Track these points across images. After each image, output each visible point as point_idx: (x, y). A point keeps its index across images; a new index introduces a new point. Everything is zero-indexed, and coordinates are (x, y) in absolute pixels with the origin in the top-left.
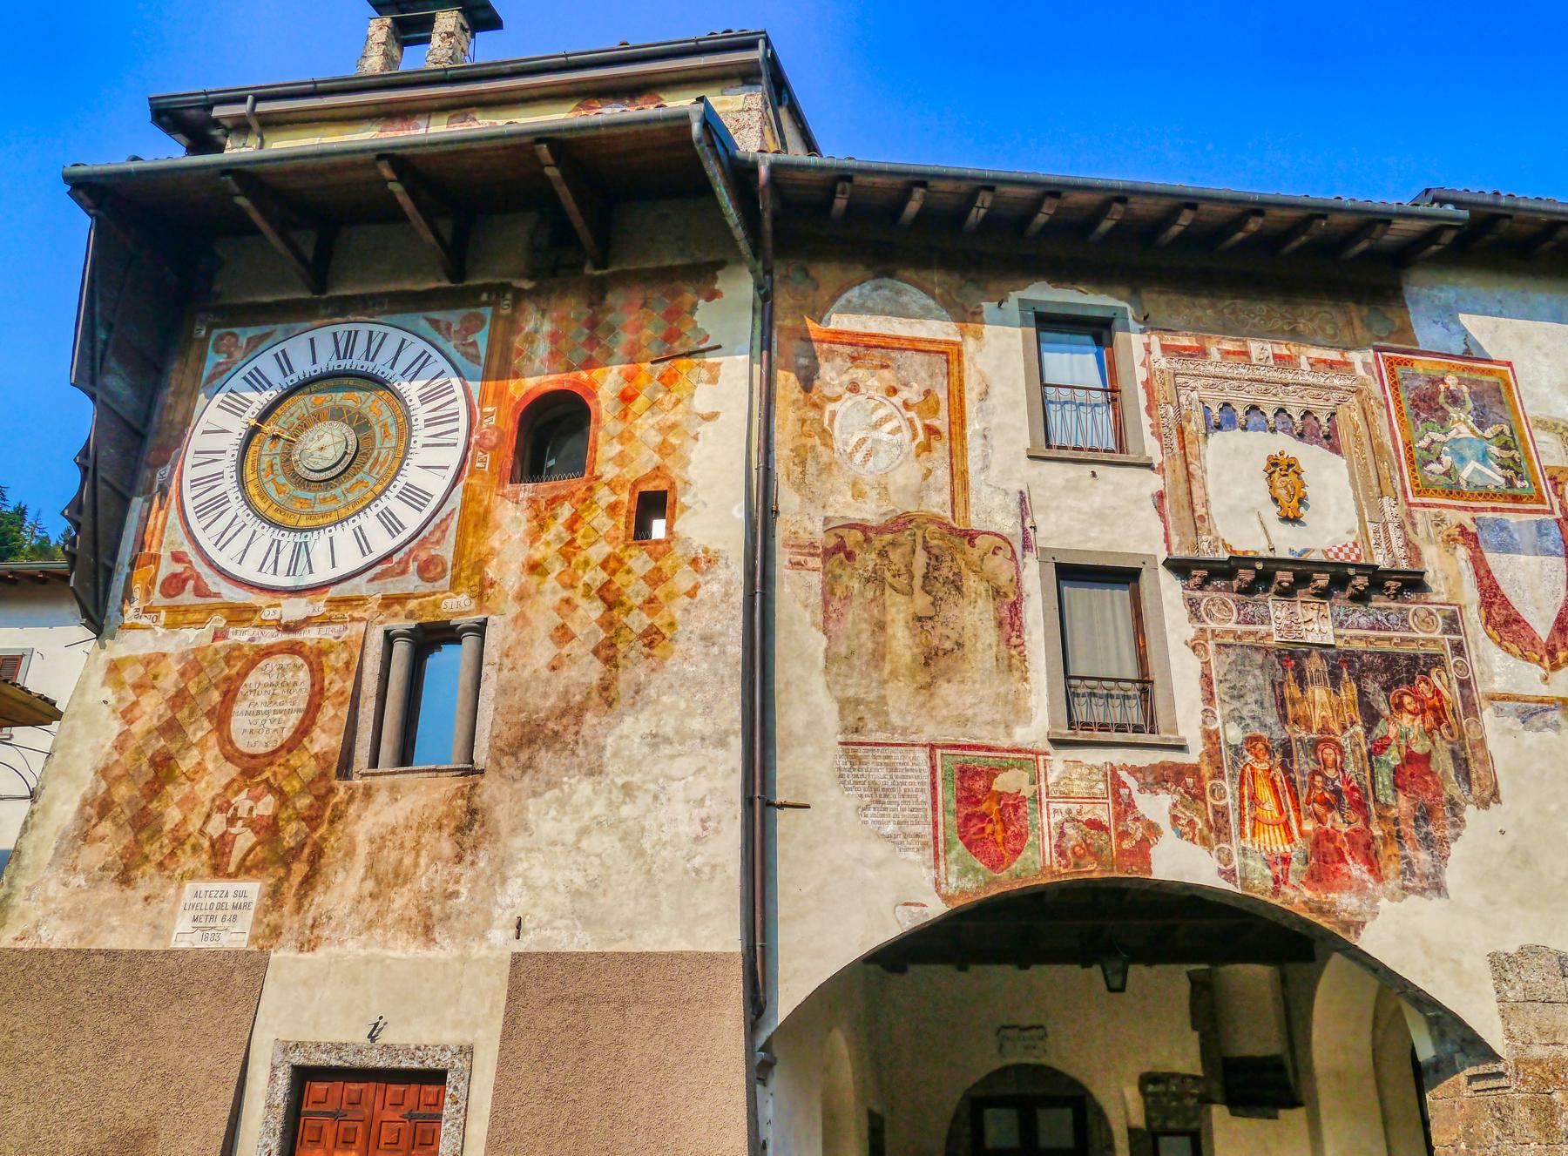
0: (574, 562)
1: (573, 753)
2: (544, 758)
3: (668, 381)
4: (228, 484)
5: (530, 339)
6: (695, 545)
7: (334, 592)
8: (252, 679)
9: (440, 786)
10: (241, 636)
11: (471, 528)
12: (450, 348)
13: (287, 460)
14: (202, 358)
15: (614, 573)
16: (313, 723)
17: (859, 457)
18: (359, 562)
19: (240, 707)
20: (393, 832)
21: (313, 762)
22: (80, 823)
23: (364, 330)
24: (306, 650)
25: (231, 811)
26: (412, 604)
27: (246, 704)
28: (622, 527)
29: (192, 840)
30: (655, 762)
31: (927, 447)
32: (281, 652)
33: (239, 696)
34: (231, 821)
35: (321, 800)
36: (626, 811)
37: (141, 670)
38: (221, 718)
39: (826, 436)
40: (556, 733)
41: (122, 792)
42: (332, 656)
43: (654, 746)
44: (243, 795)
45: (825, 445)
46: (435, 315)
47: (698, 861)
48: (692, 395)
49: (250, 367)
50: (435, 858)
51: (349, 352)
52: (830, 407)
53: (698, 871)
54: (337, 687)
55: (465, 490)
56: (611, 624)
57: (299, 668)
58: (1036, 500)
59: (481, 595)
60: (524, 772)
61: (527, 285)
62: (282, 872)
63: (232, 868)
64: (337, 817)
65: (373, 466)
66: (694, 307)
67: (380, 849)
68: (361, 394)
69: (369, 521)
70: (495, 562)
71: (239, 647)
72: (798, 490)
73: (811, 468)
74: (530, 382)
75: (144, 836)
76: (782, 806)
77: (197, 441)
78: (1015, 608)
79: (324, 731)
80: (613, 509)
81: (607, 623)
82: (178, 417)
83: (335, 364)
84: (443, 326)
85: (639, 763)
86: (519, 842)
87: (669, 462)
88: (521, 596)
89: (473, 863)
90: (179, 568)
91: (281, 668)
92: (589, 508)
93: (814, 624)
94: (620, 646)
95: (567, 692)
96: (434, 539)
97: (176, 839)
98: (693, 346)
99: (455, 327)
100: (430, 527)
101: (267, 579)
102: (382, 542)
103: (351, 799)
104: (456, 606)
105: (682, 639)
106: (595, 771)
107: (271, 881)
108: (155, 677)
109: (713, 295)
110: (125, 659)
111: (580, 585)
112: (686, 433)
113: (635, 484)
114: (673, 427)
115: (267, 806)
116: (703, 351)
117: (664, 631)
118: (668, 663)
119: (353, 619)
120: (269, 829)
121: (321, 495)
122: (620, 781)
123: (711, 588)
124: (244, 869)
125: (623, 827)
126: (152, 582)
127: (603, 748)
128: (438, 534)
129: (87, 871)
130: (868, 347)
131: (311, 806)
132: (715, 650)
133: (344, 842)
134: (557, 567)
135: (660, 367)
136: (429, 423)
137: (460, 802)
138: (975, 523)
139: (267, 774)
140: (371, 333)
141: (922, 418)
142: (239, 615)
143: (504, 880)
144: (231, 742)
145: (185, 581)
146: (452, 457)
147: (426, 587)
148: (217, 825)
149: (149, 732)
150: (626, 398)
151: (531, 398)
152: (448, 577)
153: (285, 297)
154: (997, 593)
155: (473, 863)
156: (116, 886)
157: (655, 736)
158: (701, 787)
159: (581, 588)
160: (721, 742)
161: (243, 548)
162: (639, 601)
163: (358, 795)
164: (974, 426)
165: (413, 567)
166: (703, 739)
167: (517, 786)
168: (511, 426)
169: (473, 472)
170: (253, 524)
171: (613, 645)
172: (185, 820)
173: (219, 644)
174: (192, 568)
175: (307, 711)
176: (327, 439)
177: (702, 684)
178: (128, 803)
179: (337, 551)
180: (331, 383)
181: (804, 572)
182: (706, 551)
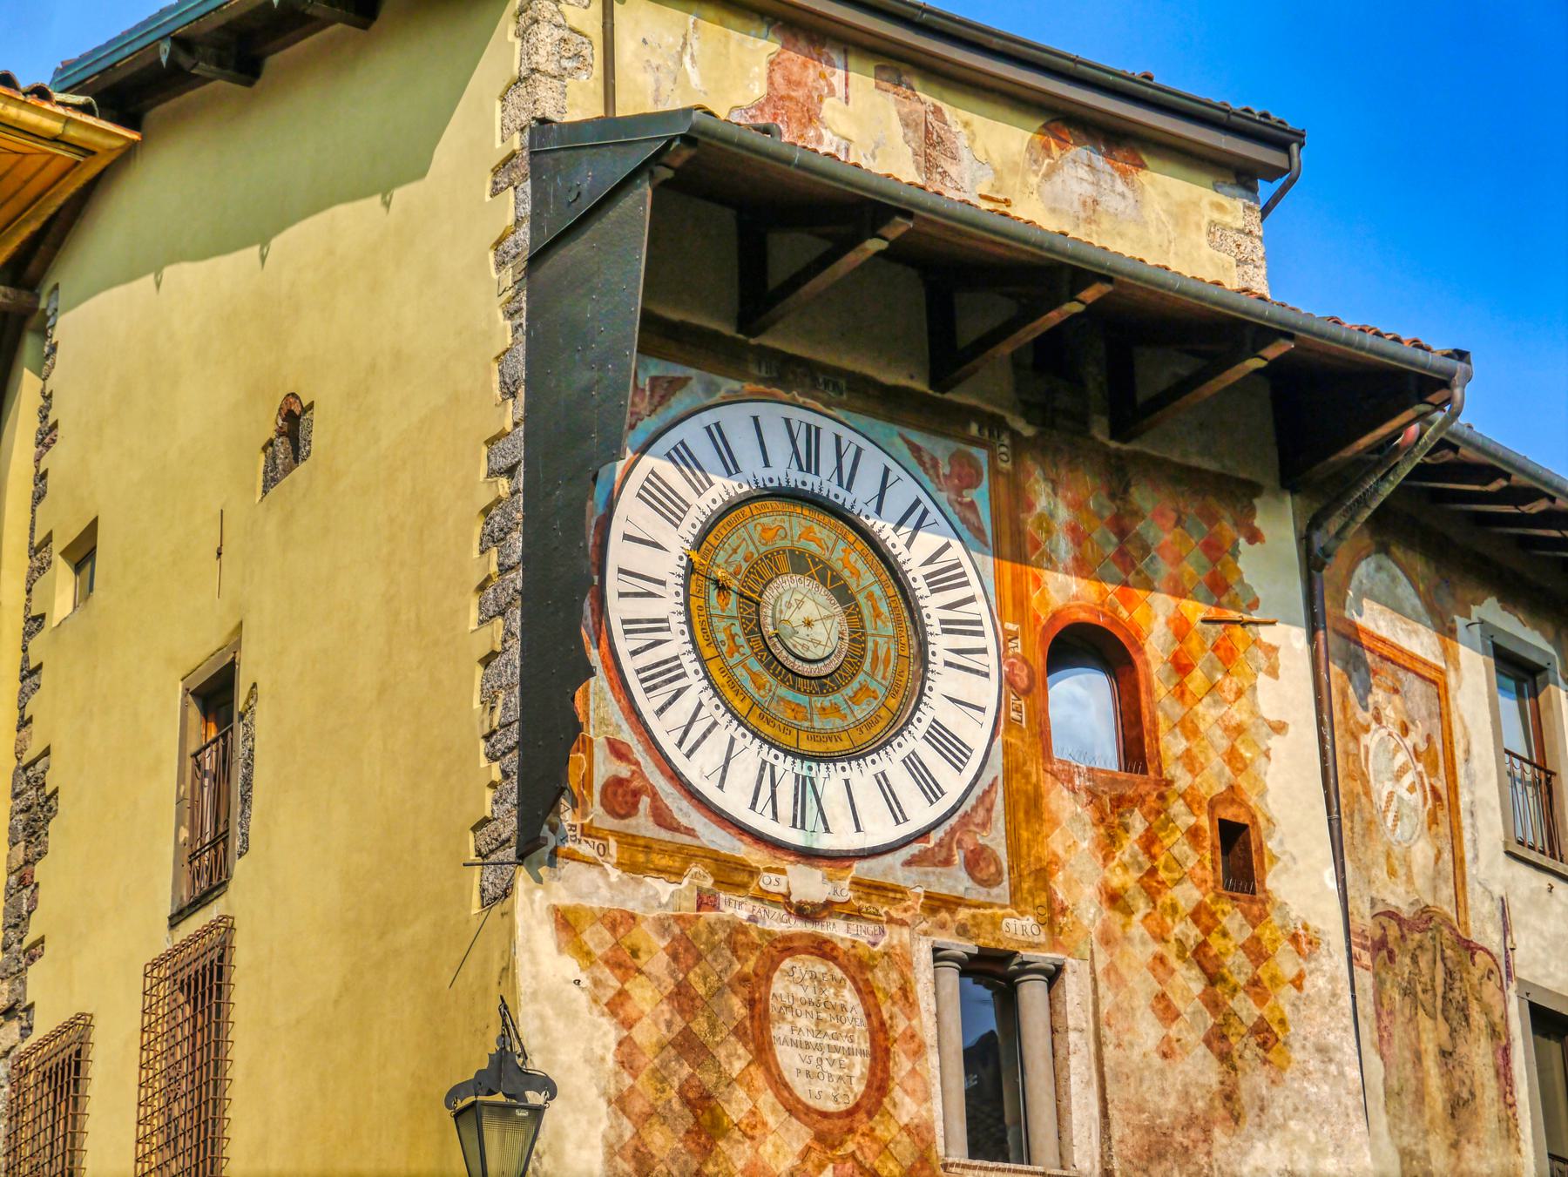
0: (1159, 903)
4: (676, 644)
6: (1293, 915)
7: (859, 869)
10: (736, 909)
11: (1021, 815)
12: (942, 497)
15: (1207, 931)
17: (1391, 816)
18: (893, 833)
19: (780, 1031)
21: (906, 1139)
23: (829, 429)
26: (963, 914)
27: (786, 1028)
31: (1433, 820)
32: (806, 951)
33: (773, 1013)
37: (607, 935)
40: (1186, 1149)
42: (879, 974)
46: (917, 438)
48: (1254, 688)
52: (1365, 739)
57: (840, 984)
58: (1513, 914)
61: (1028, 431)
70: (1060, 876)
78: (1506, 1051)
80: (1194, 834)
81: (1213, 1004)
83: (796, 478)
84: (926, 459)
87: (1242, 781)
90: (624, 771)
91: (814, 977)
92: (1164, 827)
94: (1233, 1040)
95: (1187, 1093)
99: (945, 469)
101: (761, 822)
102: (921, 814)
104: (1019, 930)
105: (1297, 1045)
108: (635, 953)
109: (1254, 537)
112: (1256, 744)
113: (1213, 805)
114: (1239, 730)
117: (1276, 1029)
118: (1287, 1075)
119: (891, 920)
123: (1317, 983)
126: (587, 782)
128: (981, 812)
132: (1333, 1068)
134: (1142, 907)
136: (949, 627)
138: (1474, 937)
139: (850, 1147)
140: (838, 438)
141: (1429, 776)
142: (731, 874)
144: (786, 1085)
145: (636, 794)
150: (1181, 667)
151: (1059, 626)
152: (1006, 883)
154: (1494, 1033)
159: (1173, 946)
162: (1242, 980)
164: (1464, 799)
165: (958, 857)
169: (1009, 721)
170: (727, 729)
171: (1224, 1037)
173: (711, 915)
174: (642, 775)
177: (1326, 1112)
182: (1306, 928)
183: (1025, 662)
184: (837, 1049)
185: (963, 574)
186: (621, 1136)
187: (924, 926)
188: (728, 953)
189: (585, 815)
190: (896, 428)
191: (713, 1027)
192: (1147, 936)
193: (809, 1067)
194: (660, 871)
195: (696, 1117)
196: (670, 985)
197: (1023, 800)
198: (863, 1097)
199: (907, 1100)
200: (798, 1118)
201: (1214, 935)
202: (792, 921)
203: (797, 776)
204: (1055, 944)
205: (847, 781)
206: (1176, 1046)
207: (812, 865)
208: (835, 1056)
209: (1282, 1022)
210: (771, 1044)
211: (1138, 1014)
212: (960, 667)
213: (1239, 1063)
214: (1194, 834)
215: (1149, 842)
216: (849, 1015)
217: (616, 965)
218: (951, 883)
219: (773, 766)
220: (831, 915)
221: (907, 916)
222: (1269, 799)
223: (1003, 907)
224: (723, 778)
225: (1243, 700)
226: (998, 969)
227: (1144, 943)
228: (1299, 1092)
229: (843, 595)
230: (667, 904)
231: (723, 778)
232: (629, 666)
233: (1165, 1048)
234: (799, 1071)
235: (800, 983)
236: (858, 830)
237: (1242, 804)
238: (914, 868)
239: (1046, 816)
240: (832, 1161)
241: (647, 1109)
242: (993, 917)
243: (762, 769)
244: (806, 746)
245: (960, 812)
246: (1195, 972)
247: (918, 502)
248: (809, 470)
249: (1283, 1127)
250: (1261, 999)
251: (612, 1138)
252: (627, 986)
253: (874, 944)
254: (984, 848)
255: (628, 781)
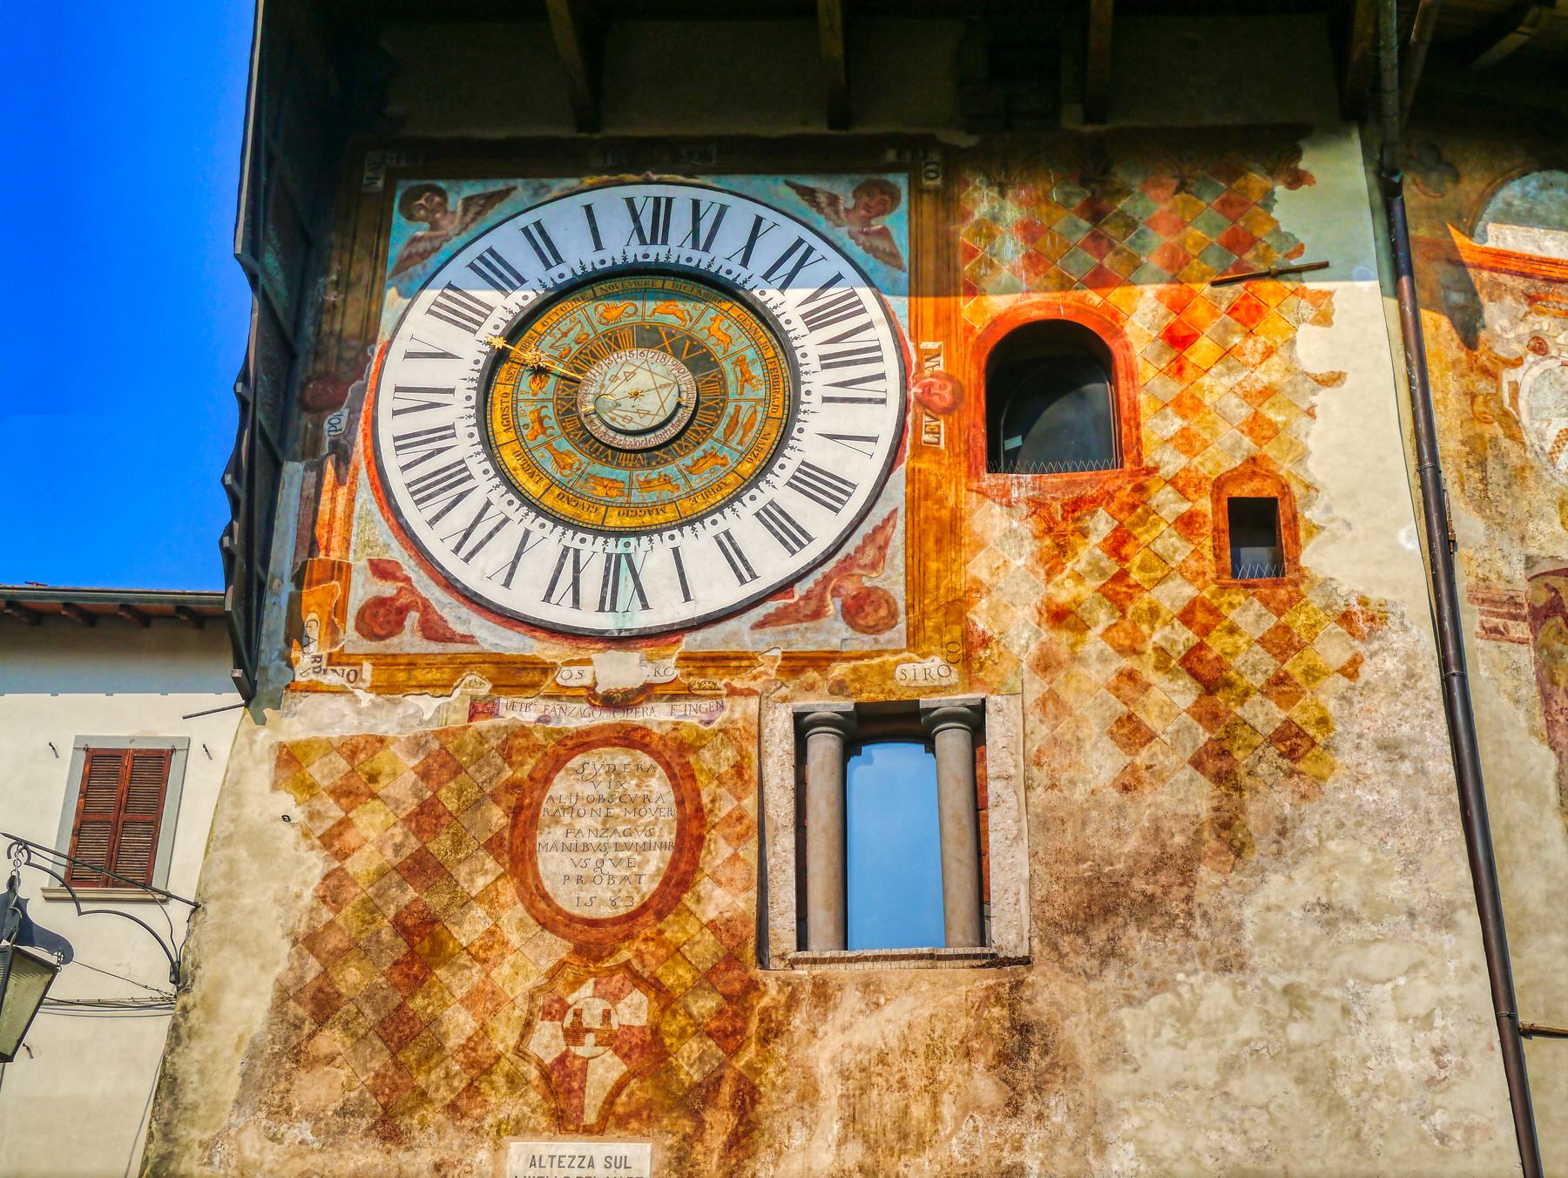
0: (1130, 610)
1: (1188, 934)
2: (1136, 940)
3: (1248, 315)
4: (465, 447)
5: (987, 230)
6: (1343, 590)
7: (690, 642)
8: (561, 787)
9: (956, 983)
10: (522, 712)
11: (930, 545)
12: (841, 235)
13: (568, 409)
14: (383, 228)
15: (1205, 631)
16: (695, 866)
18: (734, 593)
19: (549, 836)
20: (882, 1059)
21: (709, 937)
22: (282, 1030)
23: (682, 196)
24: (656, 744)
25: (569, 1019)
26: (839, 670)
27: (558, 833)
28: (1210, 556)
29: (505, 1065)
30: (1336, 951)
32: (607, 743)
34: (575, 1034)
35: (740, 998)
36: (1296, 1032)
37: (343, 765)
38: (516, 852)
39: (1510, 423)
41: (351, 977)
42: (707, 754)
43: (1331, 924)
44: (587, 990)
45: (1512, 437)
46: (809, 182)
47: (1439, 1118)
48: (1293, 342)
49: (479, 247)
50: (969, 1108)
51: (660, 231)
52: (1508, 376)
53: (1443, 1138)
54: (726, 807)
55: (911, 477)
56: (1215, 717)
57: (647, 772)
59: (967, 659)
60: (1104, 963)
61: (966, 141)
62: (688, 1126)
63: (590, 1117)
64: (772, 1033)
65: (731, 429)
66: (1268, 199)
67: (863, 1090)
68: (689, 306)
69: (743, 523)
70: (984, 603)
71: (524, 732)
72: (1480, 510)
73: (1495, 474)
74: (998, 303)
75: (410, 1055)
76: (1532, 1032)
77: (396, 371)
79: (719, 883)
80: (1187, 524)
82: (351, 324)
83: (636, 252)
84: (822, 199)
85: (1307, 953)
86: (1116, 1082)
87: (1270, 450)
88: (1045, 664)
89: (1040, 1117)
90: (388, 589)
91: (613, 771)
92: (1142, 521)
93: (1533, 732)
94: (1238, 755)
95: (1158, 829)
96: (866, 559)
97: (472, 1064)
98: (1278, 260)
100: (856, 540)
101: (561, 613)
102: (774, 564)
103: (792, 1002)
104: (923, 675)
106: (1231, 964)
107: (670, 1140)
108: (373, 778)
109: (1298, 180)
110: (308, 743)
111: (1149, 650)
112: (1292, 404)
113: (1219, 485)
114: (1268, 392)
115: (634, 1010)
116: (1298, 270)
117: (1311, 732)
118: (1329, 785)
119: (733, 692)
120: (649, 1051)
121: (641, 475)
122: (1278, 982)
123: (1383, 665)
124: (612, 1120)
125: (1297, 1059)
126: (340, 610)
127: (1240, 926)
128: (871, 551)
129: (314, 1117)
130: (1549, 280)
131: (720, 1012)
132: (1406, 767)
133: (794, 1076)
134: (1103, 618)
135: (1230, 293)
136: (828, 362)
137: (996, 1011)
139: (625, 954)
140: (696, 204)
143: (1102, 1147)
144: (545, 897)
145: (402, 612)
146: (883, 422)
147: (863, 643)
148: (547, 1041)
149: (382, 873)
151: (1002, 332)
152: (902, 625)
153: (523, 132)
155: (1040, 1117)
156: (374, 1143)
157: (1328, 907)
158: (1423, 995)
159: (1150, 657)
160: (1445, 921)
161: (516, 562)
162: (1259, 680)
163: (805, 994)
165: (833, 606)
166: (1412, 915)
167: (1094, 986)
168: (972, 375)
170: (521, 520)
171: (1225, 753)
172: (484, 1031)
173: (483, 724)
174: (413, 591)
175: (679, 847)
176: (642, 379)
177: (1393, 823)
178: (368, 998)
179: (692, 572)
180: (629, 283)
181: (1506, 646)
182: (1364, 602)
183: (950, 378)
184: (627, 847)
185: (859, 302)
186: (301, 978)
187: (784, 691)
188: (499, 761)
189: (334, 643)
190: (781, 178)
191: (458, 843)
192: (1110, 650)
193: (582, 872)
194: (423, 687)
195: (411, 946)
196: (411, 804)
197: (934, 528)
198: (653, 896)
199: (718, 892)
200: (554, 932)
201: (1214, 634)
202: (597, 713)
203: (609, 557)
204: (970, 681)
205: (676, 551)
206: (1145, 774)
207: (627, 649)
208: (623, 854)
209: (1323, 722)
210: (532, 853)
211: (1088, 746)
212: (844, 400)
213: (1248, 781)
214: (1187, 524)
215: (1118, 544)
216: (653, 806)
217: (345, 793)
218: (821, 637)
219: (577, 551)
220: (649, 699)
221: (757, 685)
222: (1311, 463)
223: (896, 652)
224: (511, 575)
225: (1275, 359)
226: (913, 727)
227: (1103, 659)
228: (1345, 804)
229: (613, 342)
230: (430, 721)
231: (511, 575)
232: (398, 483)
233: (1127, 780)
234: (567, 878)
235: (592, 780)
236: (687, 597)
237: (1269, 475)
238: (768, 630)
239: (966, 540)
240: (595, 975)
241: (345, 944)
242: (882, 666)
243: (564, 556)
244: (614, 521)
245: (840, 556)
246: (1185, 681)
247: (800, 242)
248: (654, 241)
249: (1319, 849)
250: (1287, 700)
251: (289, 980)
252: (351, 815)
253: (708, 723)
254: (870, 591)
255: (392, 599)
